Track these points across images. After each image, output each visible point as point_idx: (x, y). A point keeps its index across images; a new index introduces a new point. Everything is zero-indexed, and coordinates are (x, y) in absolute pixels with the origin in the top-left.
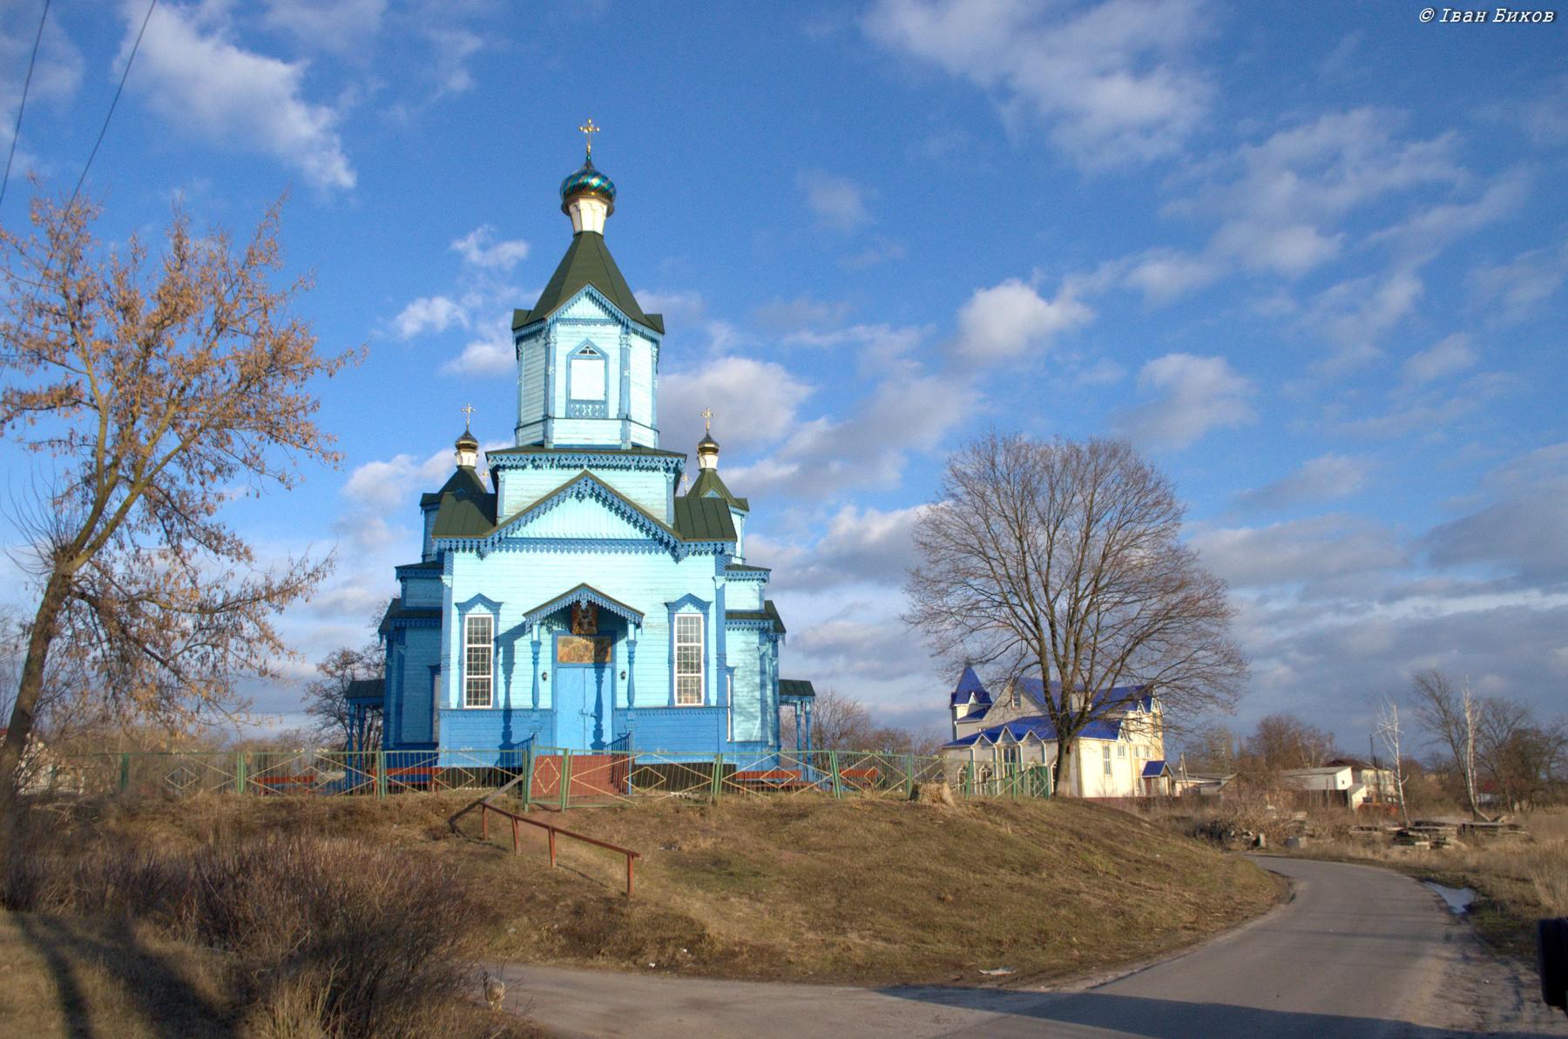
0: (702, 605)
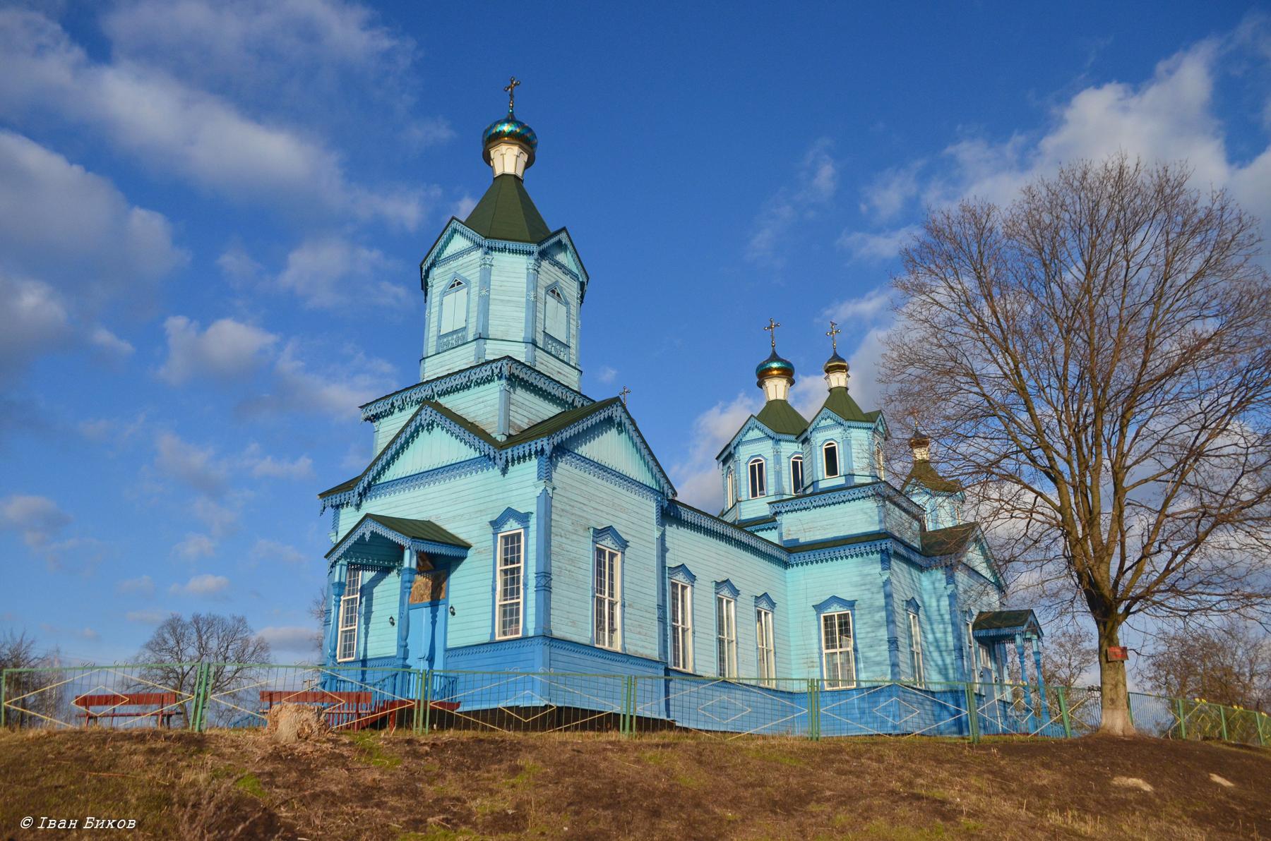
0: (524, 518)
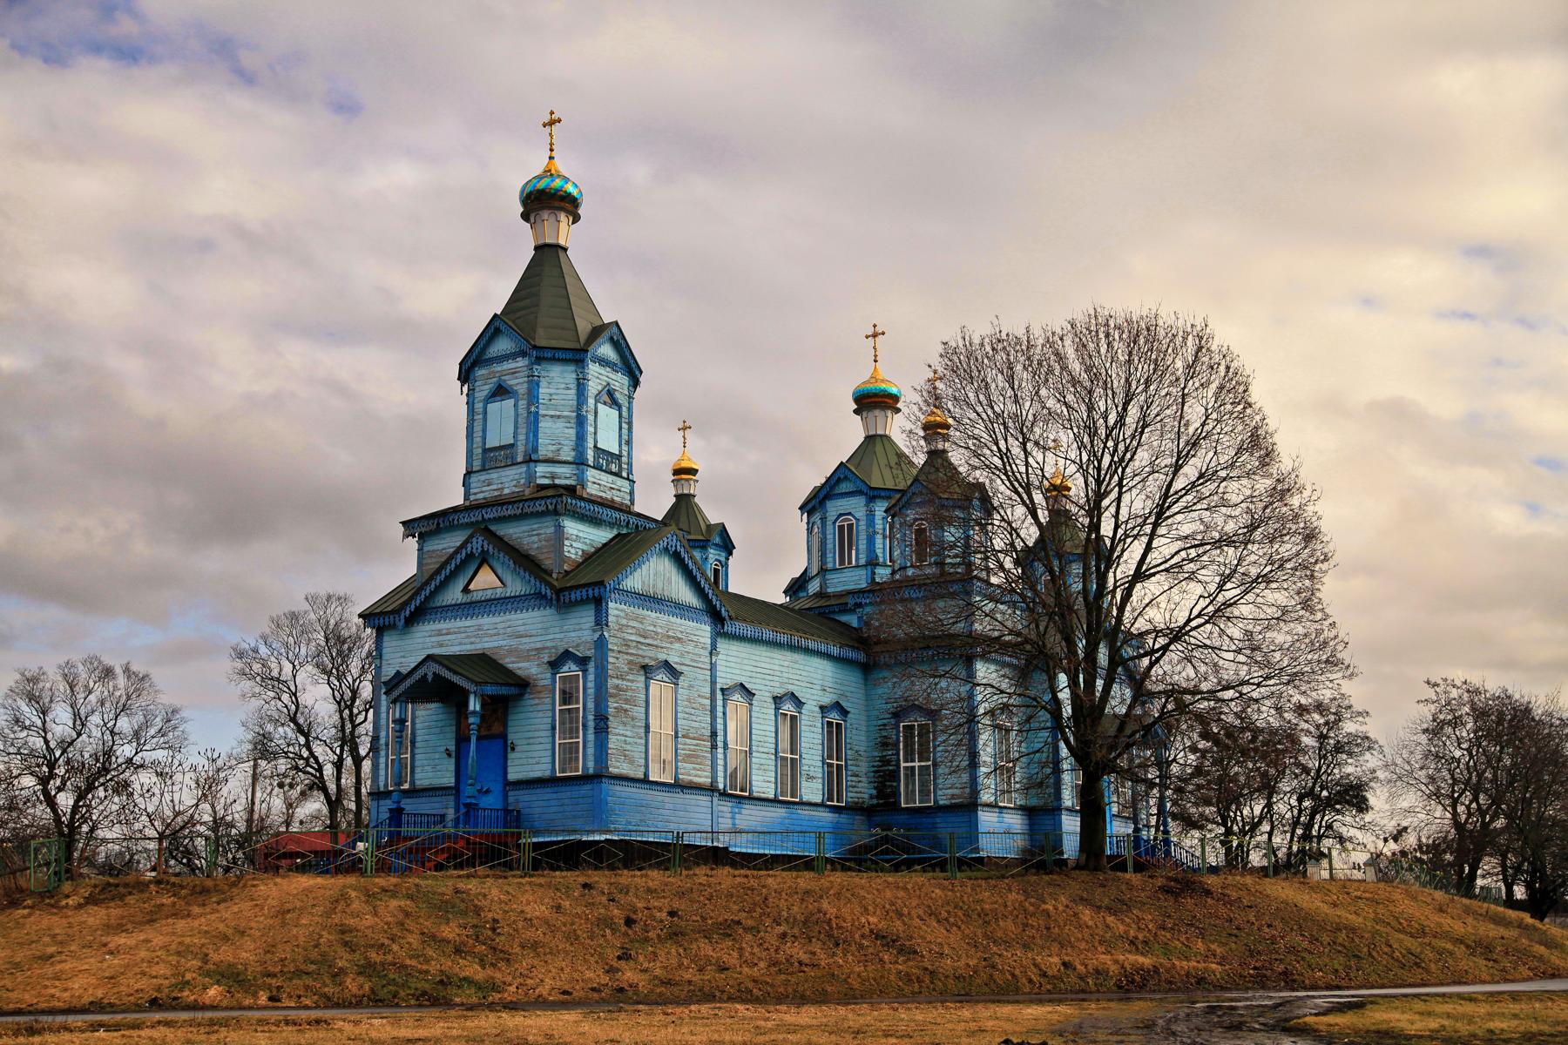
0: (583, 662)
